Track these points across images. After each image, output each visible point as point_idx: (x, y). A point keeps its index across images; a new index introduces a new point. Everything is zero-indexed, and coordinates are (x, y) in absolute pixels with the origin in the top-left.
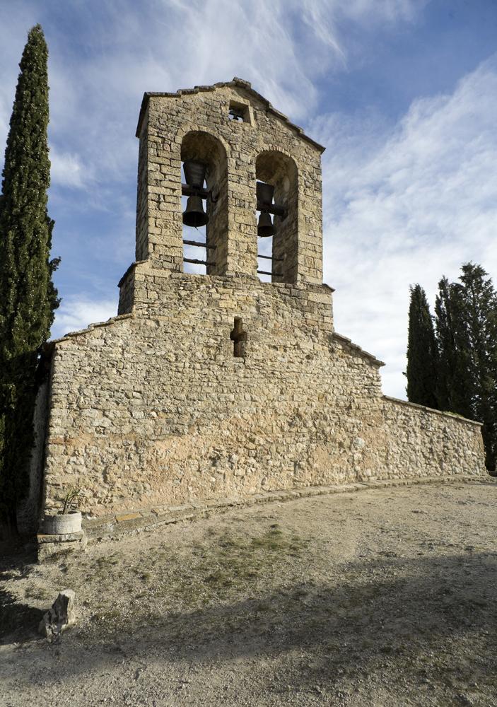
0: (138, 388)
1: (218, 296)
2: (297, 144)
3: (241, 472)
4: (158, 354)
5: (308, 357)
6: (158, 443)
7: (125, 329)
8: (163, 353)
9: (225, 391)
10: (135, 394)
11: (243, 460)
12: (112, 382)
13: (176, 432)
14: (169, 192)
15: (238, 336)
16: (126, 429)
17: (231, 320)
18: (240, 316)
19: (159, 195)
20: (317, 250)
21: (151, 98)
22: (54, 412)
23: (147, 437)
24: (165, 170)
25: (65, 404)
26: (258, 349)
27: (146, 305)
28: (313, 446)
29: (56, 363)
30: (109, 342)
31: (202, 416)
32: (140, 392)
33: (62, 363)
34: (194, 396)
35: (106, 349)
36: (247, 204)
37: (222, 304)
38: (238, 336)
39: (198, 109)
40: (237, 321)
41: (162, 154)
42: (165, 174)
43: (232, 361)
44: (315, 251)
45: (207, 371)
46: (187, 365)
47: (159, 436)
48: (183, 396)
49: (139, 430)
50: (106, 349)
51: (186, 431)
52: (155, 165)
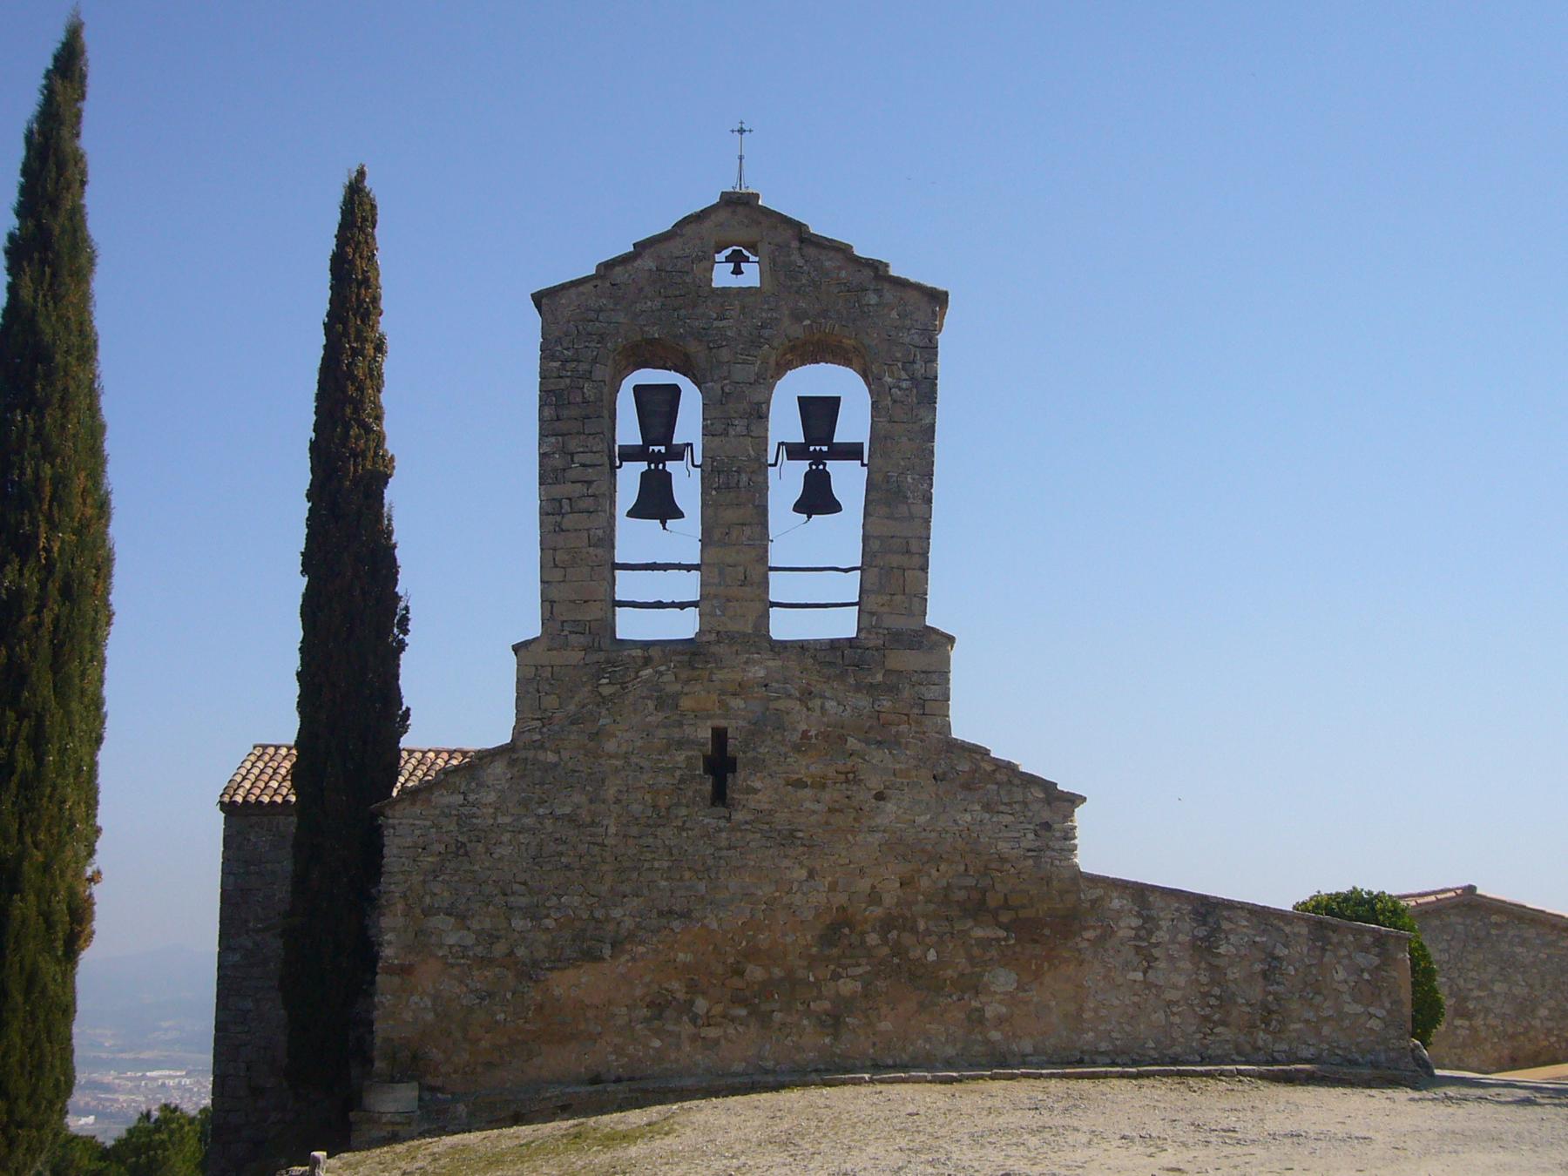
0: (522, 877)
1: (678, 687)
2: (873, 299)
3: (713, 1033)
4: (559, 812)
5: (880, 797)
6: (555, 974)
7: (499, 771)
8: (567, 810)
9: (687, 875)
10: (516, 887)
11: (718, 1009)
12: (476, 868)
13: (592, 956)
14: (579, 489)
15: (720, 763)
16: (500, 949)
17: (705, 734)
18: (722, 723)
19: (560, 501)
20: (915, 546)
21: (544, 301)
22: (385, 922)
23: (535, 964)
24: (573, 445)
25: (400, 906)
26: (757, 790)
27: (538, 724)
28: (881, 985)
29: (386, 841)
30: (472, 797)
31: (638, 926)
32: (525, 883)
33: (397, 840)
34: (626, 888)
35: (464, 810)
36: (744, 478)
37: (686, 703)
38: (720, 763)
39: (641, 290)
40: (720, 736)
41: (565, 413)
42: (572, 455)
43: (709, 819)
44: (908, 552)
45: (651, 840)
46: (612, 830)
47: (559, 962)
48: (604, 889)
49: (521, 952)
50: (464, 810)
51: (607, 952)
52: (553, 440)
